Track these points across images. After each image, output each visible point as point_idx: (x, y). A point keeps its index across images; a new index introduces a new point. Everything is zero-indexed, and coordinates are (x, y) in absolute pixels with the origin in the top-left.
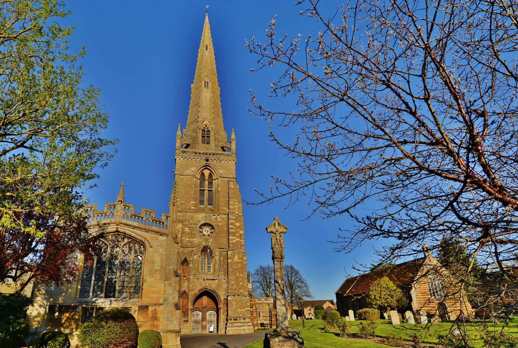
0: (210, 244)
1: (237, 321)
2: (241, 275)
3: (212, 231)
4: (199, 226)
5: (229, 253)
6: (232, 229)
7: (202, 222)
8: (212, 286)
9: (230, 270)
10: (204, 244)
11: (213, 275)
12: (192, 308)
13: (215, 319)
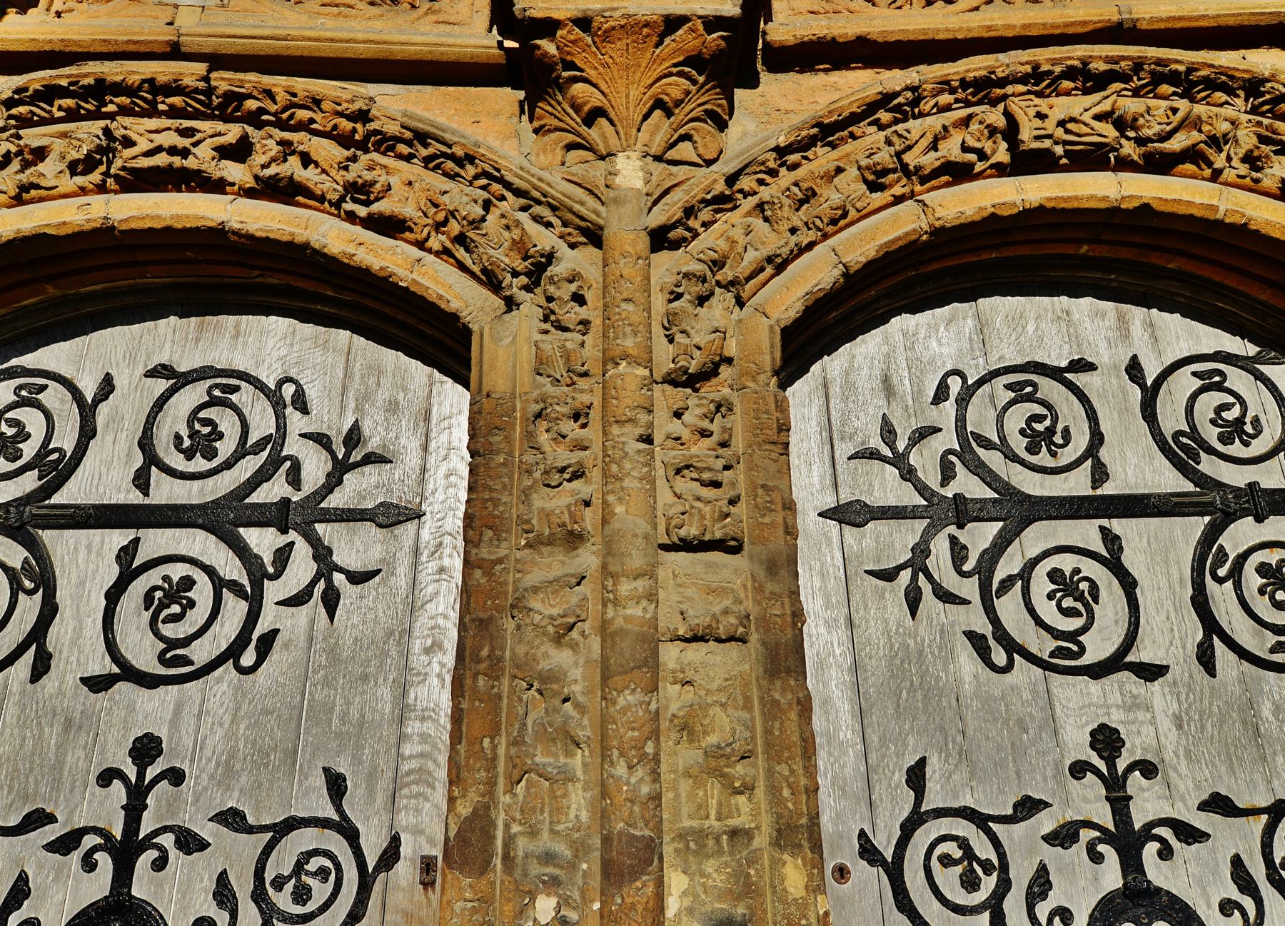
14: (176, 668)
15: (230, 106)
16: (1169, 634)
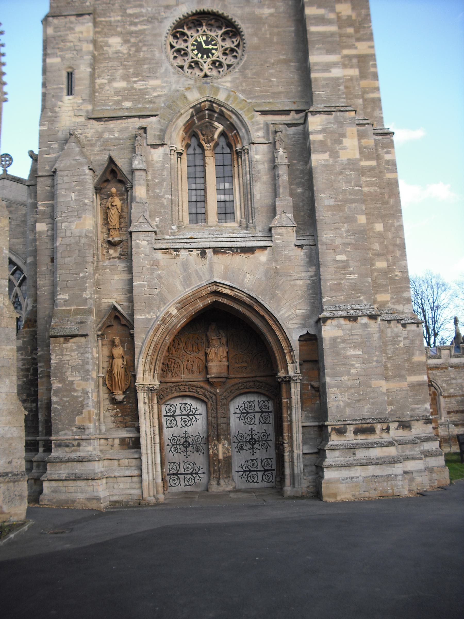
0: (221, 97)
1: (370, 438)
2: (379, 227)
3: (228, 44)
4: (169, 24)
5: (315, 123)
6: (321, 20)
7: (184, 10)
8: (245, 276)
9: (324, 199)
10: (195, 97)
11: (244, 233)
12: (156, 383)
13: (270, 429)
14: (186, 426)
15: (186, 385)
16: (257, 422)
